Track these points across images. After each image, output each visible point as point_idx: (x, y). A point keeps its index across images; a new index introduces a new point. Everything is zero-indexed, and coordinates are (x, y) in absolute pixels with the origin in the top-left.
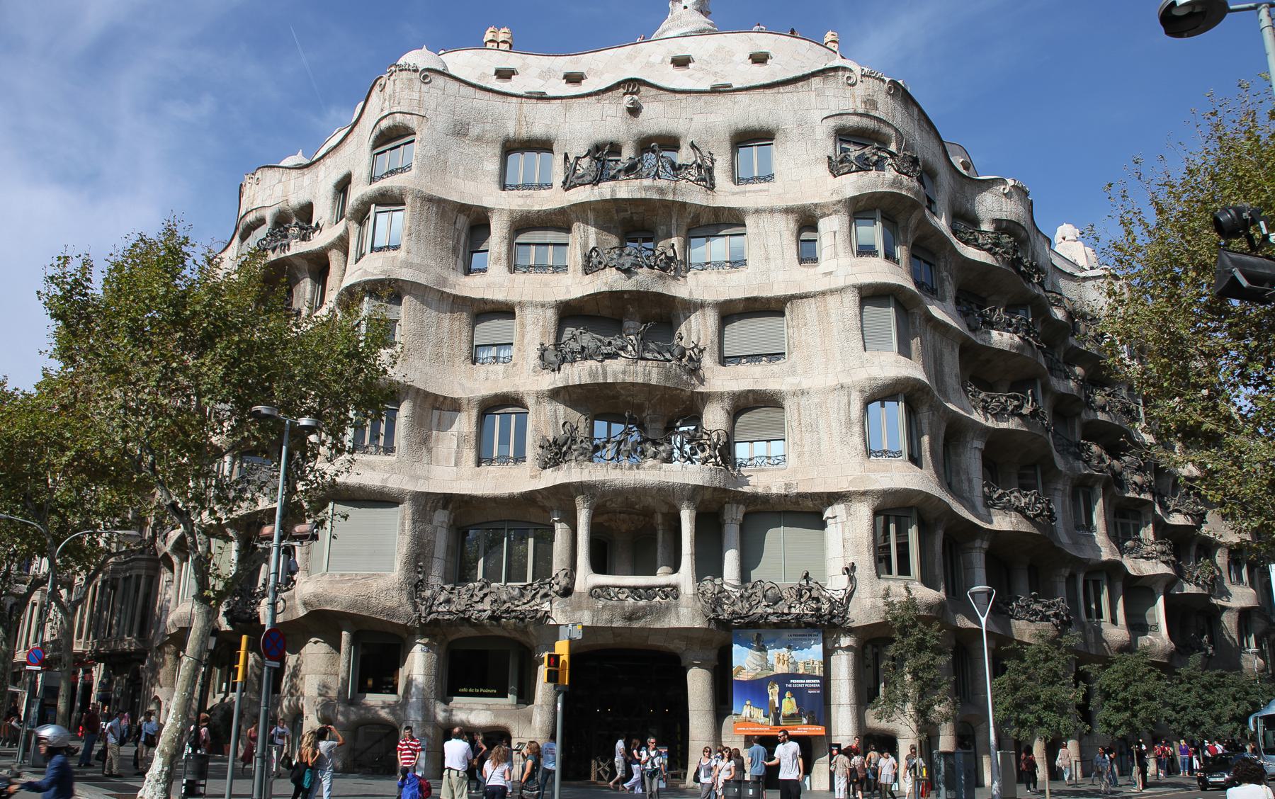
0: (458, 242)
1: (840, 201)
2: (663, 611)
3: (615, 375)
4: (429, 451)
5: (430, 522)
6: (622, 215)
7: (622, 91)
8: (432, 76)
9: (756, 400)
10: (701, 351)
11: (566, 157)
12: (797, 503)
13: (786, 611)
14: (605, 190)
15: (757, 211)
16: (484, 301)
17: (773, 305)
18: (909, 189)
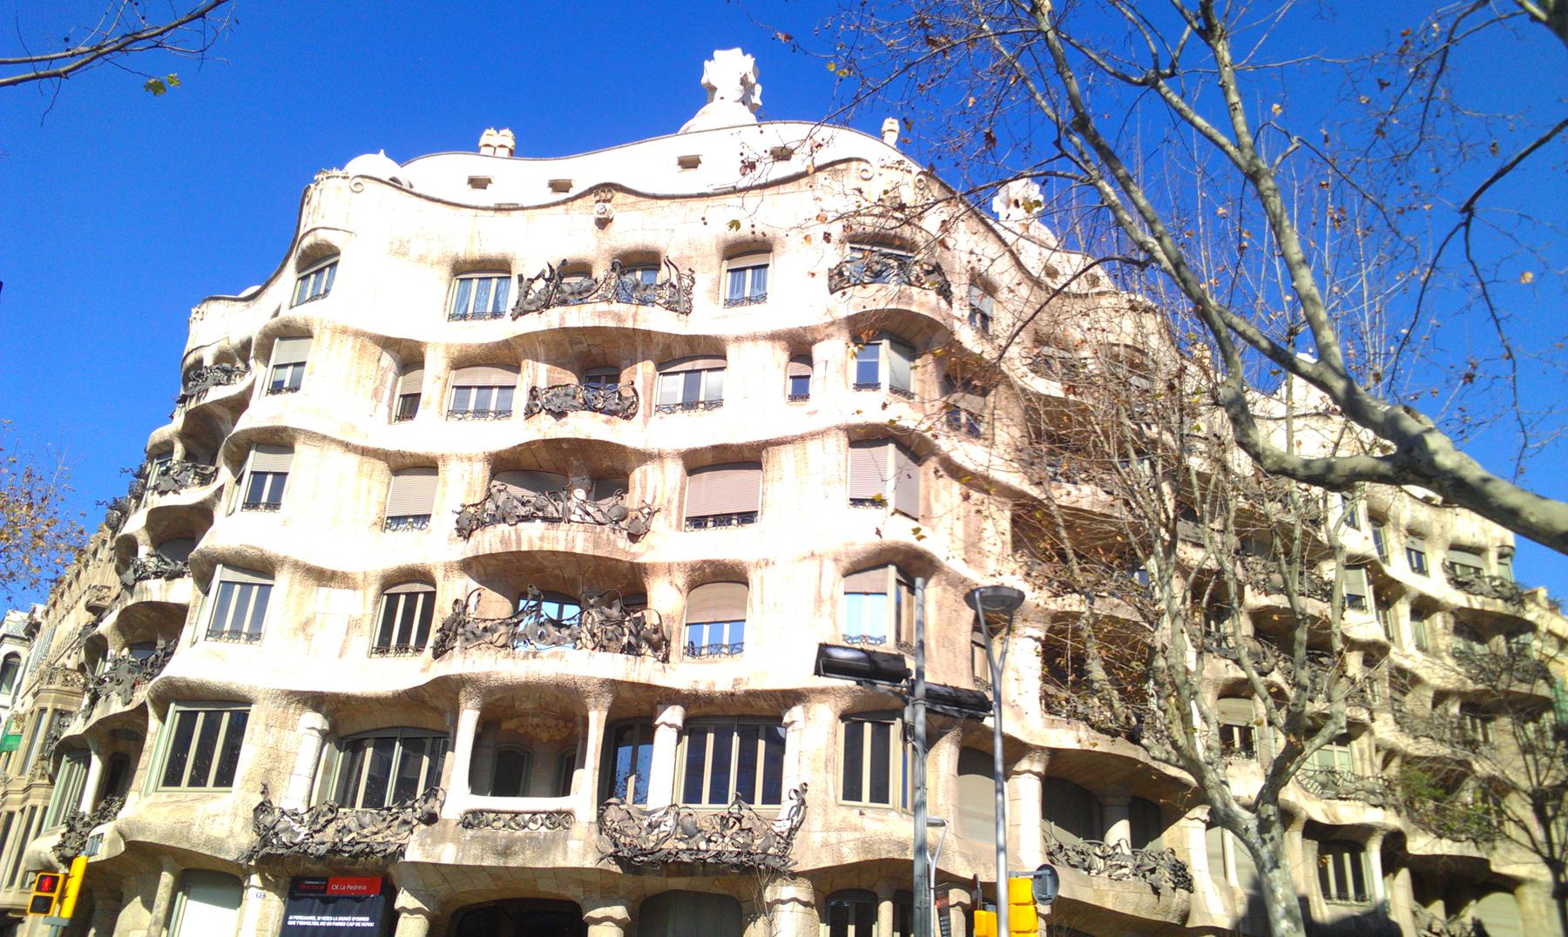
0: (383, 382)
1: (833, 323)
2: (544, 846)
3: (530, 541)
4: (309, 638)
5: (293, 729)
6: (578, 348)
7: (592, 198)
8: (367, 183)
9: (714, 574)
10: (651, 514)
11: (521, 278)
12: (748, 704)
13: (703, 845)
14: (554, 318)
15: (738, 339)
16: (402, 455)
17: (747, 454)
18: (921, 305)
